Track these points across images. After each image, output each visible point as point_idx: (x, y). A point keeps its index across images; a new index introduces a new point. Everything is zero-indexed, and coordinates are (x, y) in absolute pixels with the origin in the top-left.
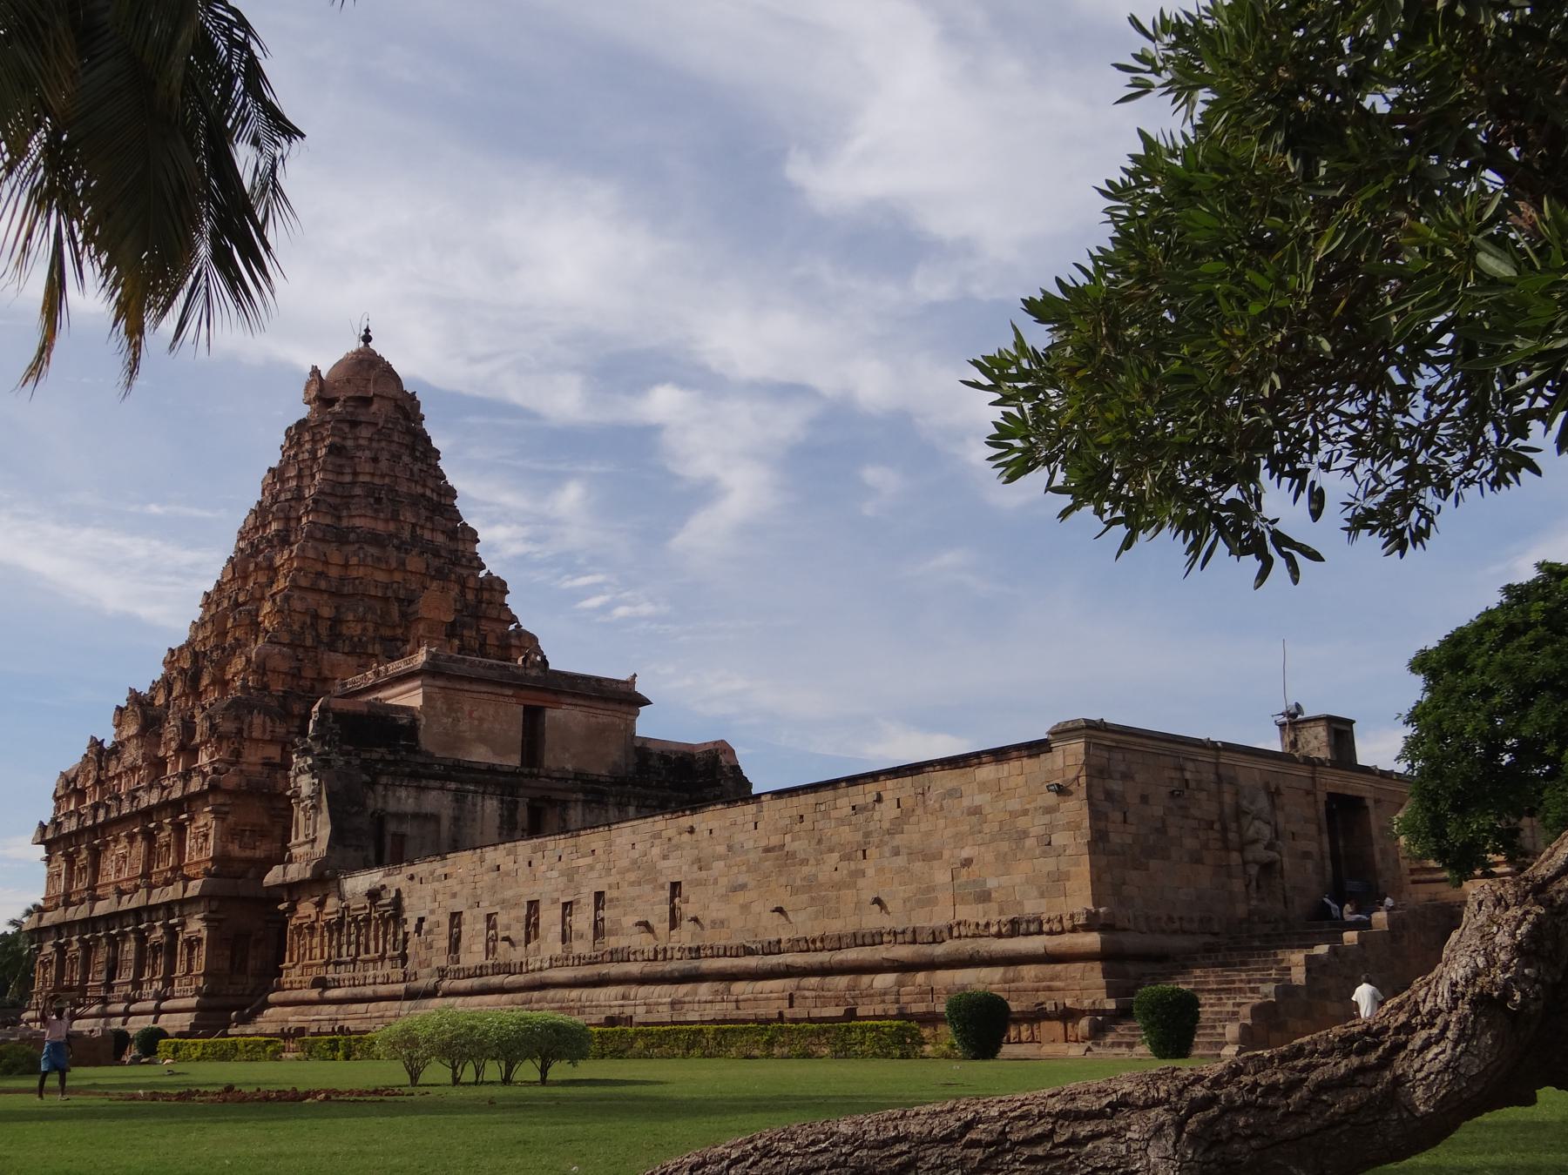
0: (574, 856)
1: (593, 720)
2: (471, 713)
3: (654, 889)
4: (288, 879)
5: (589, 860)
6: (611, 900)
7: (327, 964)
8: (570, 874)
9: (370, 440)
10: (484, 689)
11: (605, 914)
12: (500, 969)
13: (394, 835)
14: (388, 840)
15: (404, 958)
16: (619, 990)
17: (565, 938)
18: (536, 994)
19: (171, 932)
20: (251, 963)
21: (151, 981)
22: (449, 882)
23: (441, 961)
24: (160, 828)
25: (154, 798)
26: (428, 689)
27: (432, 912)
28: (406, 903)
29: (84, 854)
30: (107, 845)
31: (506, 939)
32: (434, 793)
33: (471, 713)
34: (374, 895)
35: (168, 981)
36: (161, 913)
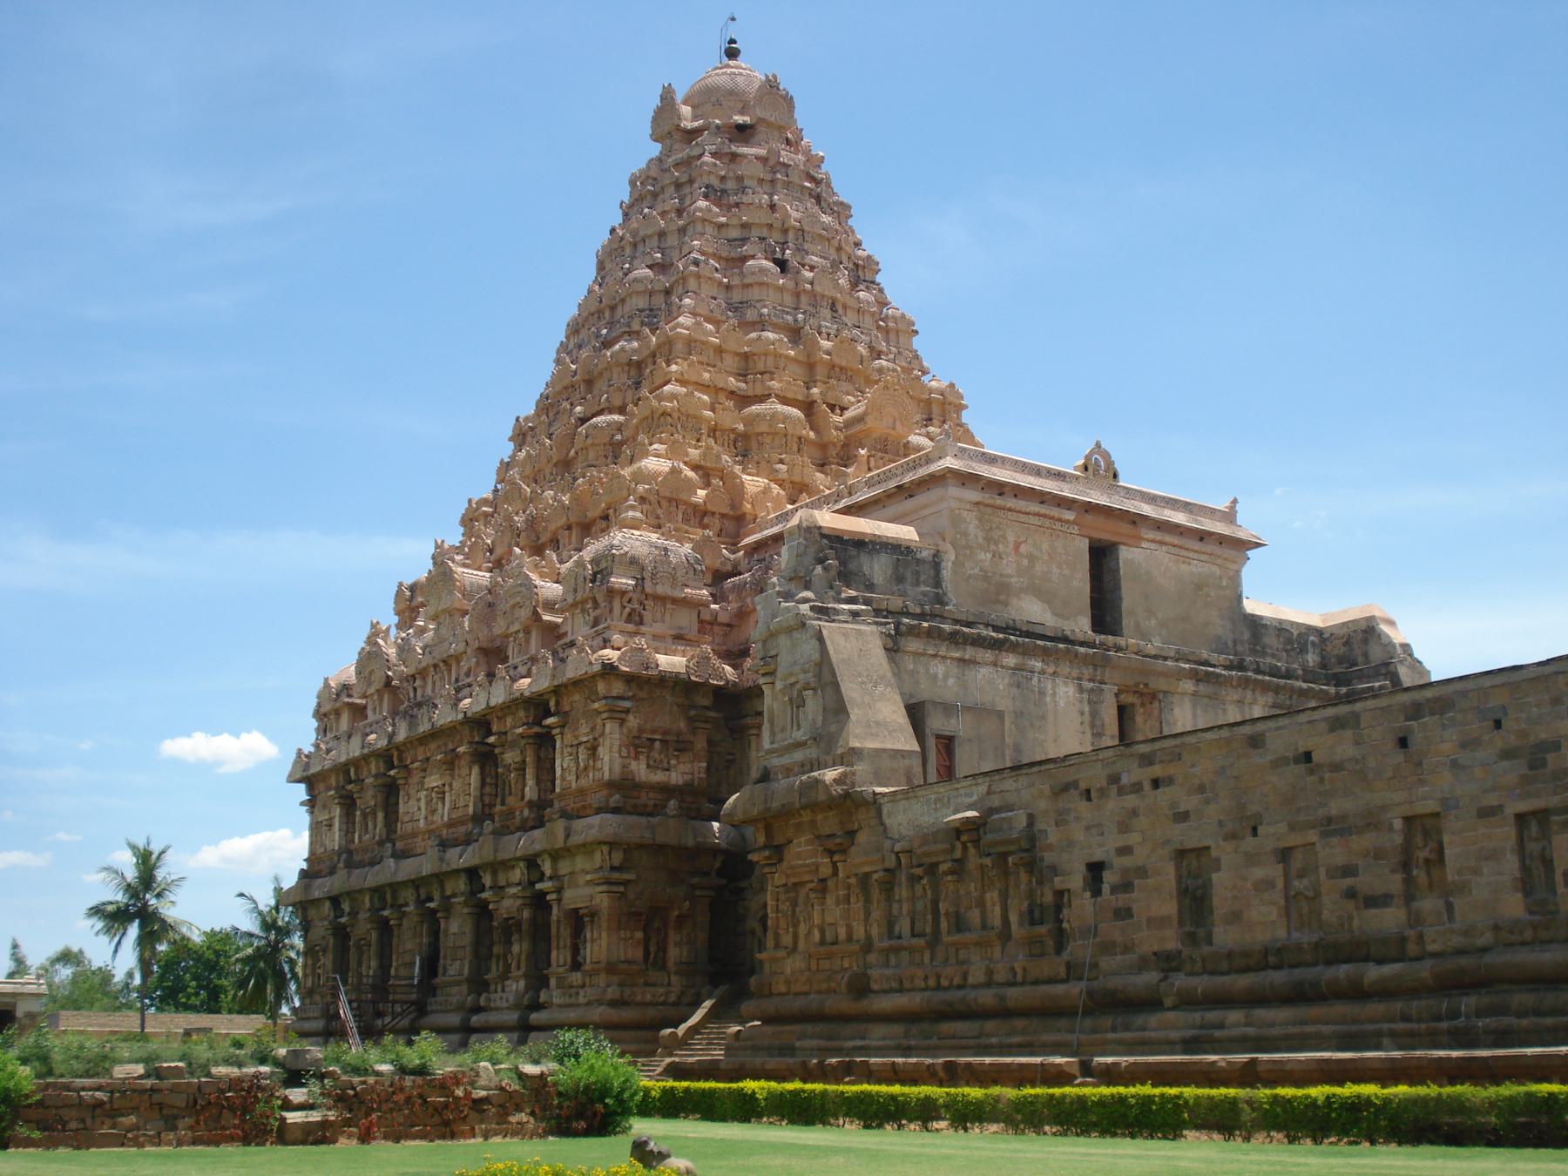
1: (1184, 567)
2: (1017, 545)
4: (775, 805)
7: (868, 947)
12: (1334, 953)
13: (938, 737)
14: (931, 743)
15: (1061, 939)
17: (1526, 885)
18: (1468, 1002)
19: (539, 902)
20: (673, 953)
21: (504, 976)
22: (1164, 794)
23: (1170, 941)
25: (498, 696)
27: (1125, 851)
28: (1053, 836)
31: (1351, 894)
32: (984, 671)
33: (1017, 545)
35: (538, 980)
36: (517, 874)
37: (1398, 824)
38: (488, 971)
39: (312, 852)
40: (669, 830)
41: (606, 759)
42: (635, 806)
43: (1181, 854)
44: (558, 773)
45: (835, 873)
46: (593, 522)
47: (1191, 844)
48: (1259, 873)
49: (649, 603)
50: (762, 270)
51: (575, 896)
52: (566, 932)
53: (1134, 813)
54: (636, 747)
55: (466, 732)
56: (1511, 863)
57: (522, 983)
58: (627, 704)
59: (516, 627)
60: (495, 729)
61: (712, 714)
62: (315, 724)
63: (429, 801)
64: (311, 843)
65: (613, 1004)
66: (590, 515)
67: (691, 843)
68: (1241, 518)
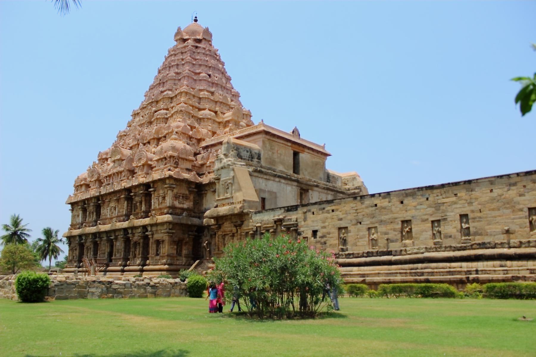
0: (440, 197)
3: (513, 211)
4: (221, 214)
5: (454, 199)
6: (474, 218)
8: (437, 206)
9: (204, 54)
10: (282, 141)
11: (472, 225)
16: (498, 263)
18: (420, 265)
19: (146, 238)
20: (184, 252)
21: (135, 256)
24: (135, 195)
26: (264, 139)
29: (91, 208)
30: (104, 202)
34: (279, 222)
36: (139, 230)
37: (400, 223)
38: (129, 255)
39: (72, 223)
40: (184, 219)
41: (168, 200)
42: (175, 213)
43: (340, 229)
44: (153, 203)
45: (237, 232)
46: (161, 138)
47: (342, 226)
48: (361, 233)
49: (180, 160)
50: (205, 77)
51: (157, 236)
52: (154, 246)
53: (327, 218)
54: (176, 197)
55: (124, 192)
56: (430, 233)
57: (140, 259)
58: (174, 186)
59: (140, 165)
60: (133, 191)
61: (195, 190)
62: (74, 188)
63: (111, 210)
64: (72, 221)
65: (168, 265)
66: (160, 136)
67: (190, 223)
68: (326, 149)
